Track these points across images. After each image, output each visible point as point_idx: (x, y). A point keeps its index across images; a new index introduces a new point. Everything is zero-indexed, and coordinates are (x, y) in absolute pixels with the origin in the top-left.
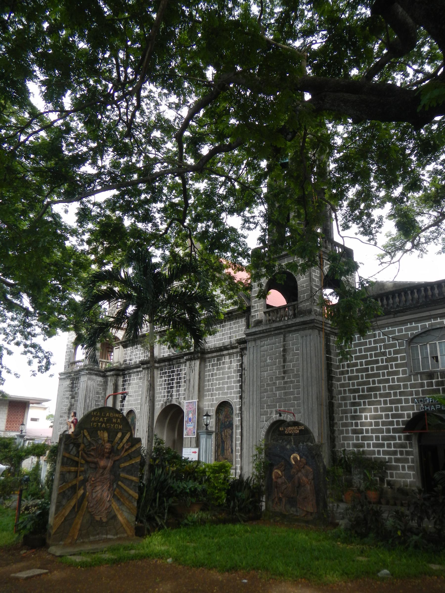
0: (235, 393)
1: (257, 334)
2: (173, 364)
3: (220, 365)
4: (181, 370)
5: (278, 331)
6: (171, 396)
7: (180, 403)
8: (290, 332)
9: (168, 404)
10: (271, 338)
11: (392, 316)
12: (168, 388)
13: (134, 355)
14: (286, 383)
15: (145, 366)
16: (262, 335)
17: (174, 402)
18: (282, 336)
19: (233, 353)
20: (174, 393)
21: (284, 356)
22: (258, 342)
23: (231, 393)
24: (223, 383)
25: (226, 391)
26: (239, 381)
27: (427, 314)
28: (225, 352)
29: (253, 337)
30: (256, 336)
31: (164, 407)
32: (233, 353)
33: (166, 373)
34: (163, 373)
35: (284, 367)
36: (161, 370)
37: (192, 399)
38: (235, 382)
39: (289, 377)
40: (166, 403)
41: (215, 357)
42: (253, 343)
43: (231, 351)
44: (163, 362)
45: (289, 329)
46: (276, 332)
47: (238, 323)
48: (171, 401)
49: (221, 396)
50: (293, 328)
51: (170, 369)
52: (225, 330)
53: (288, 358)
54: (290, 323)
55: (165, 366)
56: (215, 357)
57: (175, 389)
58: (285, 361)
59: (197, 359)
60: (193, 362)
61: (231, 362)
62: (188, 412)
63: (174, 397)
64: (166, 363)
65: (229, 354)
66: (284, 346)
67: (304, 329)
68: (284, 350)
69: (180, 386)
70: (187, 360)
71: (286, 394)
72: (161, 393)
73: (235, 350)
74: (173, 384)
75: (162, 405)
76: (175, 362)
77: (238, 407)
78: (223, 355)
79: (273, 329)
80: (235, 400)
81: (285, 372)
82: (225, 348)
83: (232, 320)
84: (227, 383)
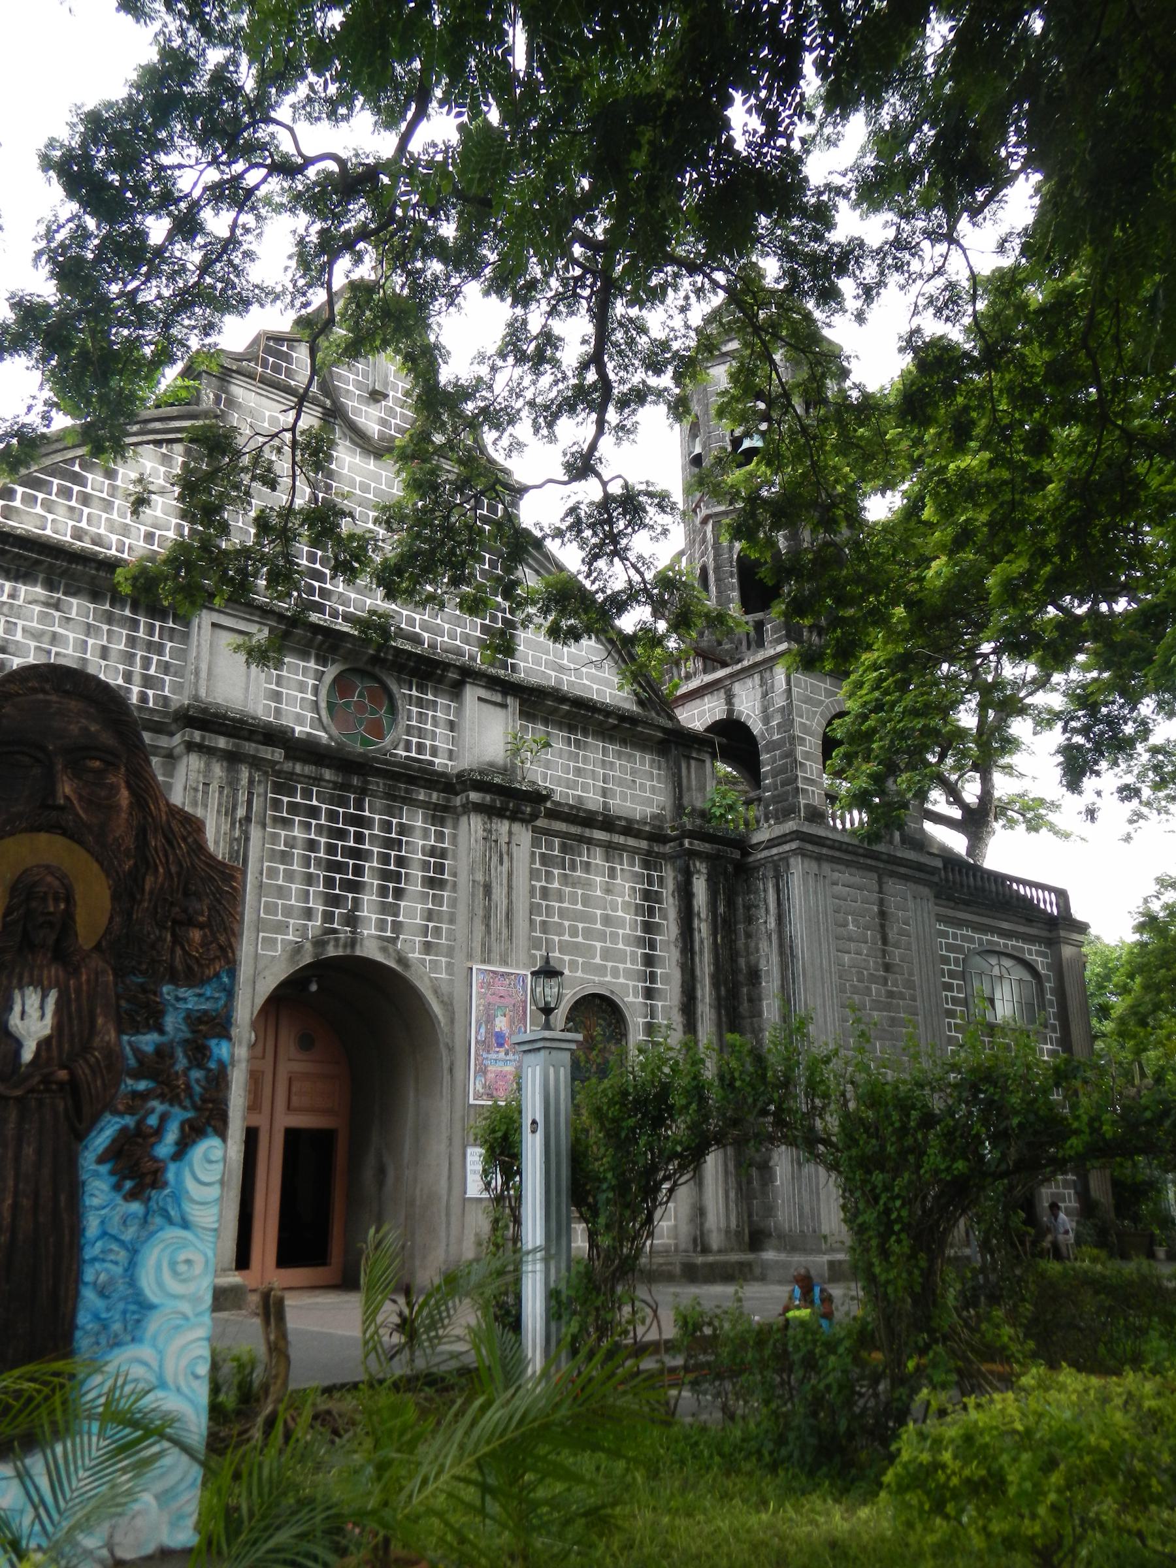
0: (628, 974)
1: (823, 846)
2: (363, 792)
3: (573, 868)
4: (403, 830)
5: (873, 863)
6: (352, 920)
7: (402, 960)
8: (893, 874)
9: (331, 952)
10: (853, 870)
11: (952, 904)
12: (329, 883)
13: (36, 635)
14: (891, 994)
15: (222, 742)
16: (837, 854)
17: (370, 950)
18: (875, 876)
19: (623, 848)
20: (369, 912)
21: (883, 926)
22: (826, 868)
23: (615, 973)
24: (588, 933)
25: (598, 960)
26: (640, 942)
27: (1005, 925)
28: (599, 835)
29: (816, 849)
30: (824, 851)
31: (307, 959)
32: (623, 848)
33: (313, 812)
34: (294, 808)
35: (884, 951)
36: (279, 788)
37: (504, 962)
38: (627, 940)
39: (895, 985)
40: (319, 943)
41: (557, 834)
42: (813, 866)
43: (621, 839)
44: (305, 761)
45: (895, 868)
46: (869, 861)
47: (631, 758)
48: (353, 943)
49: (579, 974)
50: (902, 870)
51: (343, 803)
52: (586, 760)
53: (892, 935)
54: (899, 854)
55: (318, 780)
56: (557, 834)
57: (369, 899)
58: (885, 941)
59: (523, 821)
60: (503, 827)
61: (612, 873)
62: (488, 1006)
63: (369, 931)
64: (328, 774)
65: (610, 849)
66: (881, 902)
67: (917, 881)
68: (882, 914)
69: (399, 893)
70: (479, 808)
71: (893, 1021)
72: (281, 892)
73: (631, 842)
74: (358, 871)
75: (298, 949)
76: (377, 784)
77: (641, 1020)
78: (590, 841)
79: (861, 851)
80: (630, 999)
81: (887, 968)
82: (608, 822)
83: (612, 740)
84: (602, 937)
